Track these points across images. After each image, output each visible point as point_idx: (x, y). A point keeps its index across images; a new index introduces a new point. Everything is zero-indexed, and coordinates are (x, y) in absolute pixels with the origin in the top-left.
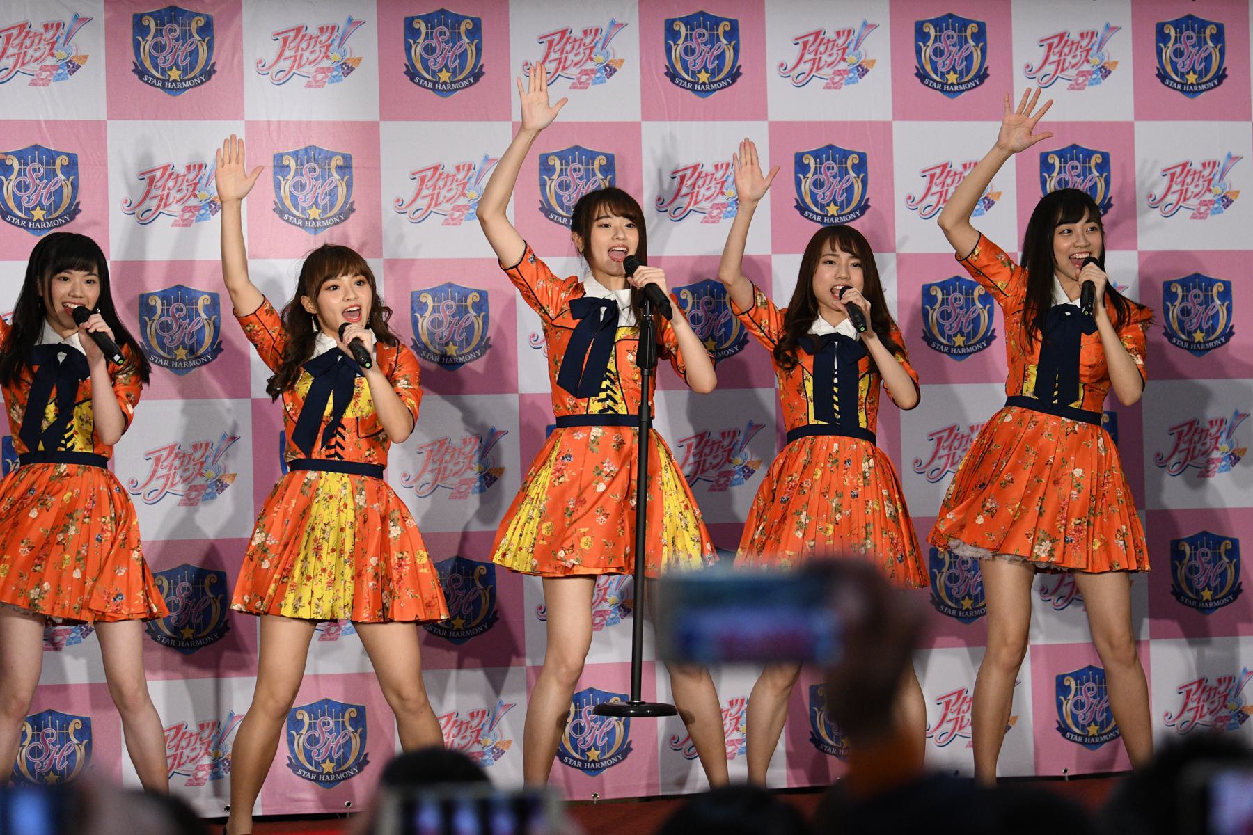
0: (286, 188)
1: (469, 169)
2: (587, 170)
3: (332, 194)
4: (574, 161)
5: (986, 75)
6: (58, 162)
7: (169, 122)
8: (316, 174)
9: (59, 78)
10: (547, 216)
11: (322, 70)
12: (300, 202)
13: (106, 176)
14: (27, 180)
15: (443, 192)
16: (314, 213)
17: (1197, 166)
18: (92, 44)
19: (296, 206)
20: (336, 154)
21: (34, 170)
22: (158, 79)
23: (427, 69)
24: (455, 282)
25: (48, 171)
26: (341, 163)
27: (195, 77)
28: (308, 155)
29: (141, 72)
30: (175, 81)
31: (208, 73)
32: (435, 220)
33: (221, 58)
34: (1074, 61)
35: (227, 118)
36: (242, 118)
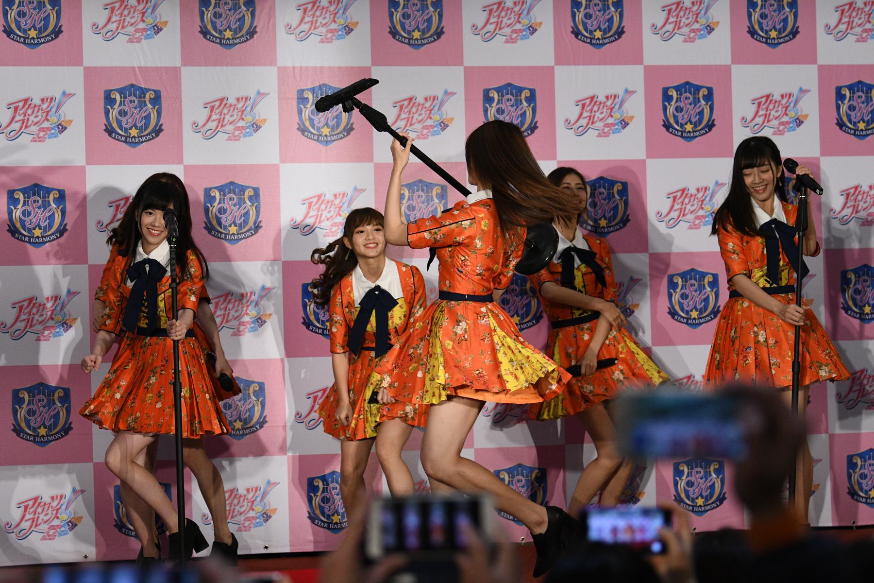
2: (516, 100)
4: (507, 94)
5: (797, 32)
6: (147, 96)
7: (225, 68)
9: (148, 37)
11: (331, 31)
12: (316, 123)
13: (181, 105)
14: (126, 109)
17: (777, 97)
18: (170, 13)
19: (313, 127)
21: (131, 102)
22: (216, 37)
23: (404, 30)
24: (424, 179)
27: (242, 36)
29: (205, 33)
30: (228, 39)
31: (252, 33)
33: (260, 23)
34: (509, 22)
35: (265, 65)
36: (275, 65)
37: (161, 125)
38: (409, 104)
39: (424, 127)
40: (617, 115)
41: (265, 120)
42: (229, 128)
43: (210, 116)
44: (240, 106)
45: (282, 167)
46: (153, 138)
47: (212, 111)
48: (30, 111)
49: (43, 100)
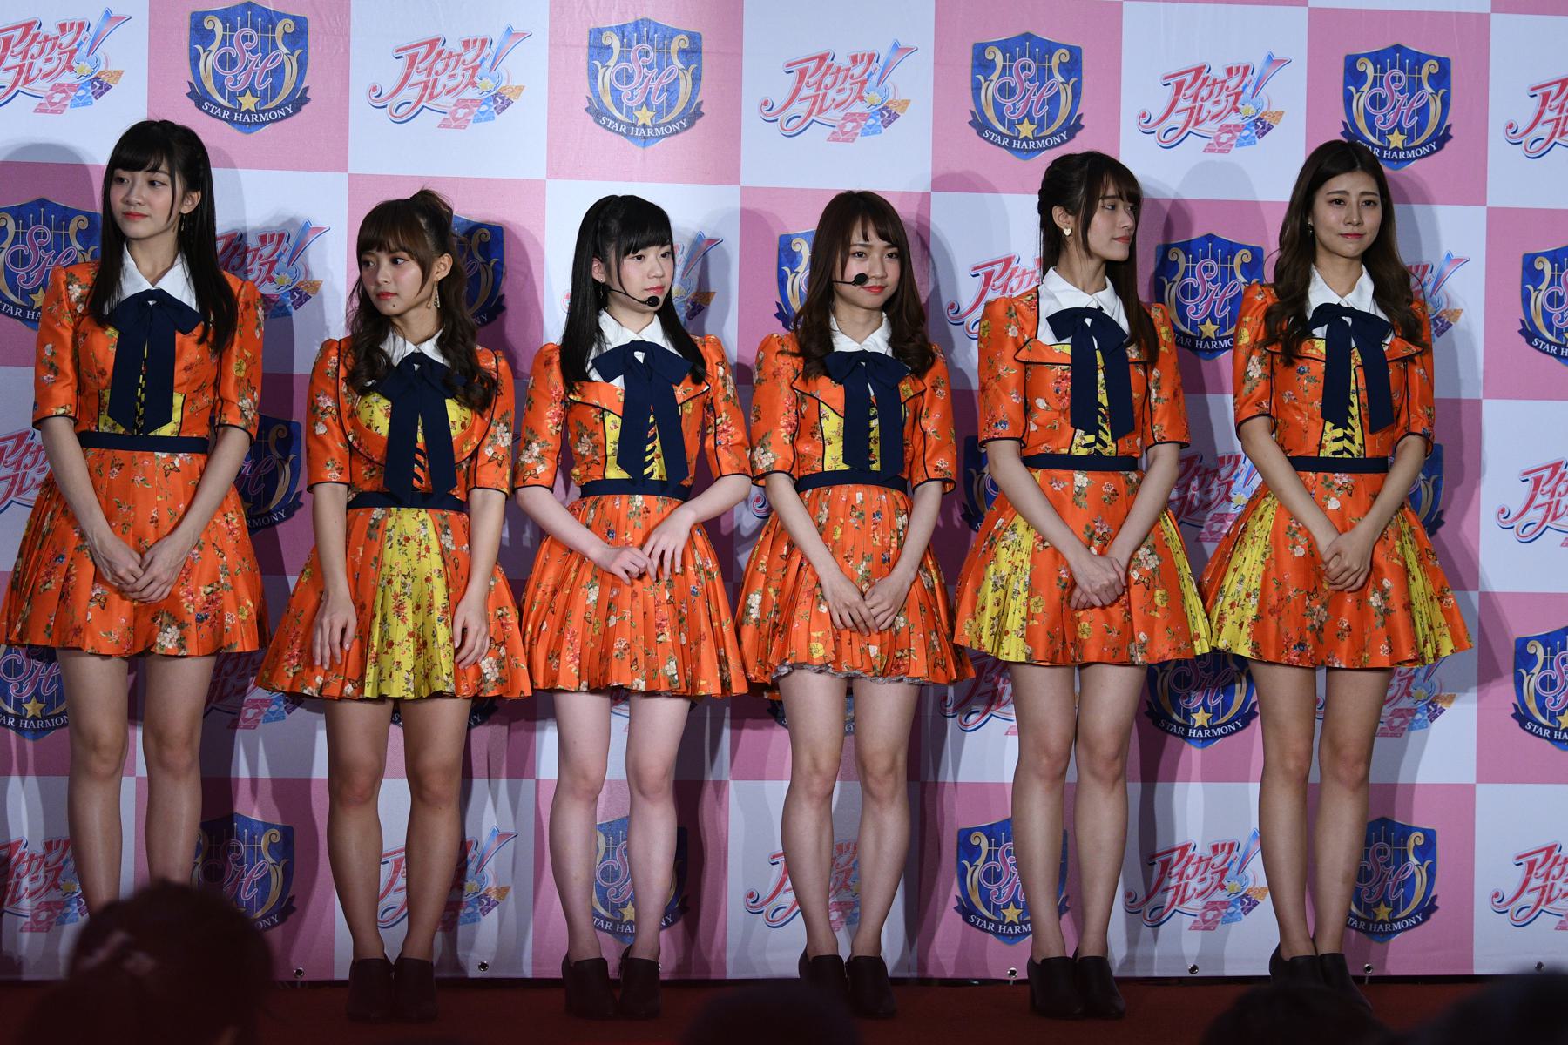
0: (606, 78)
1: (870, 62)
2: (1041, 69)
3: (671, 89)
4: (1023, 55)
6: (279, 28)
8: (648, 61)
10: (980, 133)
13: (347, 52)
15: (832, 93)
16: (644, 116)
19: (619, 106)
20: (679, 32)
21: (245, 38)
25: (264, 41)
26: (686, 46)
28: (637, 32)
32: (817, 133)
37: (306, 89)
38: (818, 69)
39: (850, 117)
40: (1248, 108)
41: (521, 88)
42: (446, 102)
43: (407, 76)
44: (469, 56)
45: (550, 183)
46: (288, 115)
47: (411, 64)
48: (35, 49)
49: (63, 27)
